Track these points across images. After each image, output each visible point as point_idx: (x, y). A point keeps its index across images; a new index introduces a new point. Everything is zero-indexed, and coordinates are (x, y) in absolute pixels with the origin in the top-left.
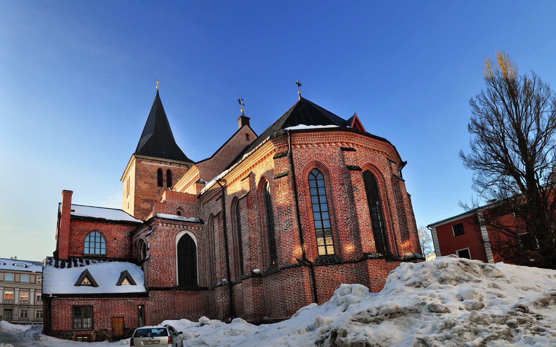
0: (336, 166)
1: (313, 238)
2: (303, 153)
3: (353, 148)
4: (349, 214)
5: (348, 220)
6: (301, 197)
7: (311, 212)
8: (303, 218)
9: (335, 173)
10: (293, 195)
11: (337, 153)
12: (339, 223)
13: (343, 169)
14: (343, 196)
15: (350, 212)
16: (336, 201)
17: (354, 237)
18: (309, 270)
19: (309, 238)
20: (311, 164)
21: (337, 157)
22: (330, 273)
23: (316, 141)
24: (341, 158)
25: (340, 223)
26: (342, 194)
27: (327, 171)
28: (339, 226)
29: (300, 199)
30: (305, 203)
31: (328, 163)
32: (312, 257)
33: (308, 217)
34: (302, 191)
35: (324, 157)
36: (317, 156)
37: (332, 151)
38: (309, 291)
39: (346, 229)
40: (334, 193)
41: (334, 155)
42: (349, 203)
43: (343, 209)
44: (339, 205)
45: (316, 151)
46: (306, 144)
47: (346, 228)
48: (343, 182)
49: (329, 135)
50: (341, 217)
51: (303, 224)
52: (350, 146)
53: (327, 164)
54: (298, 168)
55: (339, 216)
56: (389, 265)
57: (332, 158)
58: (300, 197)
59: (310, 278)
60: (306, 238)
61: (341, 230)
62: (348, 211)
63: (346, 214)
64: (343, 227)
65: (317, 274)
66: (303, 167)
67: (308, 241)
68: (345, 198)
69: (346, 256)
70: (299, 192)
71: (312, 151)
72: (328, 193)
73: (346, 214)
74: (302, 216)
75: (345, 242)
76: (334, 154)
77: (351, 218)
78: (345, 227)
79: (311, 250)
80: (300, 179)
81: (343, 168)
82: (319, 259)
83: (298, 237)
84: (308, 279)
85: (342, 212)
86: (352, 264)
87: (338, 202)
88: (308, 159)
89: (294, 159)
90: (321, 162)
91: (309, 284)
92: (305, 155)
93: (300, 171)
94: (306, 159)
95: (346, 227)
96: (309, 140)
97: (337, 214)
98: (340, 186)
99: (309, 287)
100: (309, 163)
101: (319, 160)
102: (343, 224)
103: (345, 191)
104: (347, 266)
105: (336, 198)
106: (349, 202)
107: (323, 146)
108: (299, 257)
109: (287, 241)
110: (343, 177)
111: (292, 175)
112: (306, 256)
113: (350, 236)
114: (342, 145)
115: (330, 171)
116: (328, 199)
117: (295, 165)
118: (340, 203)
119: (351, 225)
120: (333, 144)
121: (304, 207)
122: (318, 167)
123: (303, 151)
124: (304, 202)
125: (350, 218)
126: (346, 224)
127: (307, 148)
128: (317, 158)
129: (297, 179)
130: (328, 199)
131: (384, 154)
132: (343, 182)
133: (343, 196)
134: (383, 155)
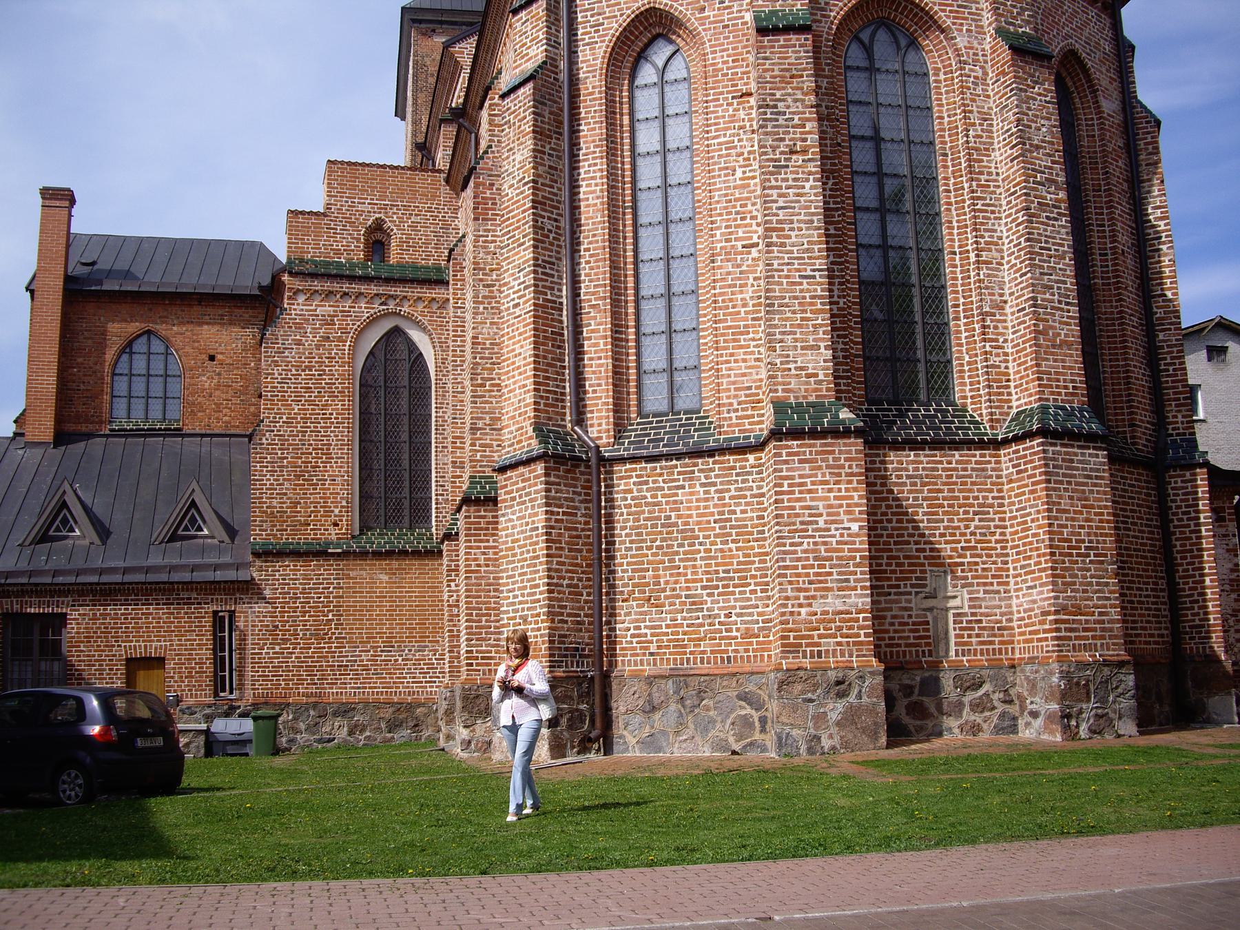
4: (754, 227)
5: (749, 253)
25: (720, 267)
34: (594, 141)
39: (740, 296)
43: (734, 207)
44: (720, 189)
47: (741, 292)
48: (746, 84)
54: (588, 44)
62: (755, 213)
63: (746, 226)
64: (730, 286)
66: (606, 35)
67: (596, 352)
73: (746, 226)
75: (732, 355)
78: (735, 286)
85: (728, 220)
87: (719, 176)
102: (729, 273)
103: (751, 126)
108: (550, 419)
110: (747, 66)
113: (754, 326)
118: (725, 182)
124: (596, 185)
126: (741, 273)
132: (746, 84)
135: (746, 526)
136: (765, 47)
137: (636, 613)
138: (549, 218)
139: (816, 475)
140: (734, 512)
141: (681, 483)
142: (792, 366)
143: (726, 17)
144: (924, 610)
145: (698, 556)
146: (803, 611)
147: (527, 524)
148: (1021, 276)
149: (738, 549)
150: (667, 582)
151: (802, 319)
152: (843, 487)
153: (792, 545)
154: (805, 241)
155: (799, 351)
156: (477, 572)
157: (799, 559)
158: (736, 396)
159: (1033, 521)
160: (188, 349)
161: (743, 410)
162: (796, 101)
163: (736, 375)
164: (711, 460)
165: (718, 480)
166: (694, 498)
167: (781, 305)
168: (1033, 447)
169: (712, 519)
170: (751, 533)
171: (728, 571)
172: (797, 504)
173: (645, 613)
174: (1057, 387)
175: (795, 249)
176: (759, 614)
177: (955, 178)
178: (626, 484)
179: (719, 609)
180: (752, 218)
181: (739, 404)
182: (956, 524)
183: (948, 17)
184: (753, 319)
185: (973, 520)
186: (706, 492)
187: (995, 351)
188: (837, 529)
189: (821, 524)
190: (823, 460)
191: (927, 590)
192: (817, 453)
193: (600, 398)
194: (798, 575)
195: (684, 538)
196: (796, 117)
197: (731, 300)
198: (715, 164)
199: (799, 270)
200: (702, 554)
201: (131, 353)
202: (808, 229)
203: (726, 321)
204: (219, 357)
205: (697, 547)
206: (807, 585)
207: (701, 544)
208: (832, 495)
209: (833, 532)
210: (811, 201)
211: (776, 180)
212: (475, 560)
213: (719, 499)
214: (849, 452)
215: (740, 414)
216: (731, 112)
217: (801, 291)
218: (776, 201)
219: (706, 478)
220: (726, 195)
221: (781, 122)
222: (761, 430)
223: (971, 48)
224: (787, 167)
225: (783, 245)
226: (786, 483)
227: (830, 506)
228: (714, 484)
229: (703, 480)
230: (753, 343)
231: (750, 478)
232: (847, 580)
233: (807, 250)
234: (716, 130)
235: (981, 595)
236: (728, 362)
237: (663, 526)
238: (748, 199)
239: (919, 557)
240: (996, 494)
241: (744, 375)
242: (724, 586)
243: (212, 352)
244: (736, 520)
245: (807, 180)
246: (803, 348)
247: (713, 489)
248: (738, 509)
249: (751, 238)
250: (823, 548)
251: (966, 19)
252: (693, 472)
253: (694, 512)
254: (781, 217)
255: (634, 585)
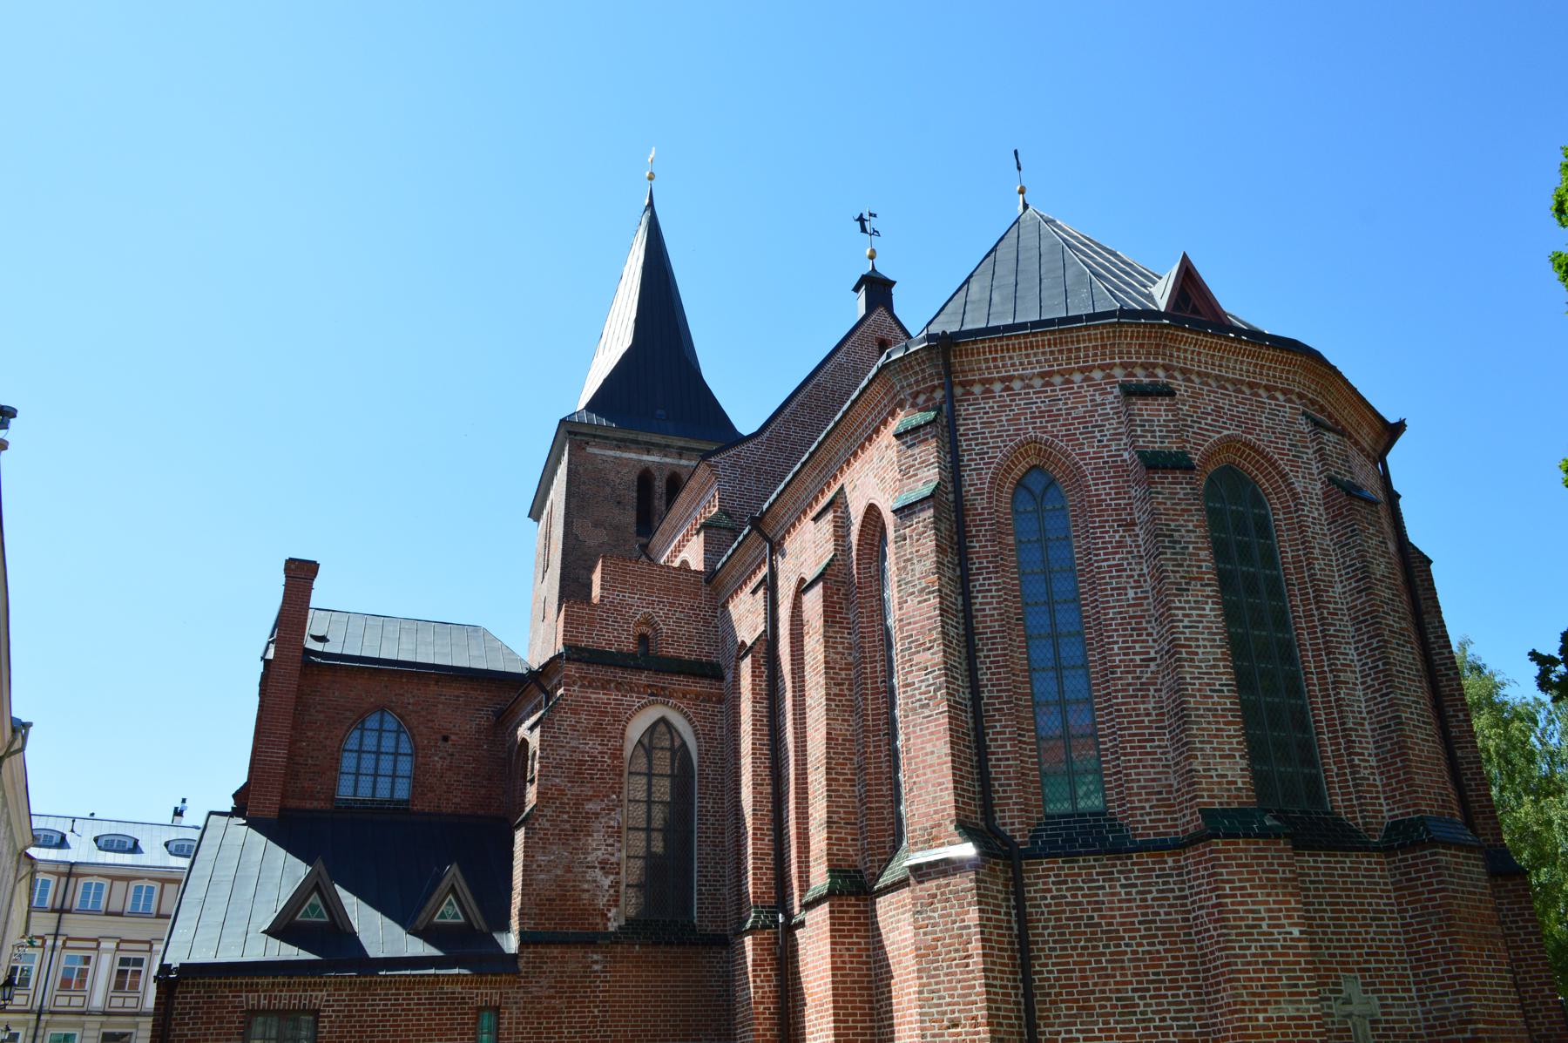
0: (1105, 454)
1: (1025, 743)
2: (991, 414)
3: (1166, 385)
4: (1151, 643)
5: (1148, 666)
6: (984, 579)
7: (1018, 636)
8: (988, 660)
9: (1103, 484)
10: (954, 570)
11: (1108, 407)
12: (1113, 679)
13: (1132, 464)
14: (1131, 570)
15: (1155, 637)
16: (1106, 590)
17: (1172, 738)
18: (1007, 872)
19: (1010, 739)
20: (1021, 453)
21: (1108, 419)
22: (1083, 889)
23: (1035, 368)
24: (1122, 423)
25: (1120, 679)
26: (1125, 563)
27: (1076, 474)
28: (1116, 691)
29: (978, 588)
30: (994, 600)
31: (1077, 445)
32: (1016, 820)
33: (1005, 655)
34: (987, 557)
35: (1063, 425)
36: (1041, 422)
37: (1091, 401)
38: (1002, 965)
39: (1142, 706)
40: (1096, 561)
41: (1099, 415)
42: (1151, 600)
43: (1130, 624)
44: (1114, 607)
45: (1036, 403)
46: (1002, 380)
47: (1144, 703)
48: (1129, 514)
49: (1078, 342)
50: (1122, 657)
51: (986, 686)
52: (1156, 376)
53: (1074, 450)
54: (974, 470)
55: (1116, 651)
56: (1320, 868)
57: (1092, 427)
58: (978, 580)
59: (1008, 907)
60: (996, 740)
61: (1123, 708)
62: (1150, 630)
63: (1143, 641)
64: (1132, 696)
65: (1036, 891)
66: (992, 463)
67: (1003, 753)
68: (1136, 578)
69: (1144, 822)
70: (977, 558)
71: (1022, 402)
72: (1081, 558)
73: (1143, 641)
74: (985, 653)
75: (1140, 760)
76: (1097, 411)
77: (1158, 661)
78: (1137, 696)
79: (1014, 791)
80: (980, 511)
81: (1129, 462)
82: (1045, 830)
83: (969, 735)
84: (999, 913)
85: (1125, 636)
86: (1166, 858)
87: (1112, 595)
88: (1007, 436)
89: (961, 435)
90: (1053, 441)
91: (1003, 935)
92: (998, 421)
93: (980, 479)
94: (1002, 436)
95: (1143, 696)
96: (1013, 365)
97: (1109, 643)
98: (1121, 533)
99: (1005, 950)
100: (1012, 447)
101: (1045, 436)
102: (1129, 684)
103: (1139, 552)
104: (1147, 863)
105: (1104, 578)
106: (1150, 595)
107: (1063, 383)
109: (926, 754)
110: (1130, 498)
111: (951, 497)
112: (998, 815)
113: (1159, 734)
114: (1126, 376)
115: (1086, 476)
116: (1081, 582)
117: (966, 458)
118: (1118, 601)
119: (1160, 690)
120: (1097, 375)
121: (993, 615)
122: (1045, 463)
123: (991, 404)
124: (992, 597)
125: (1154, 659)
126: (1141, 684)
127: (1005, 394)
128: (1040, 428)
129: (968, 510)
130: (1081, 582)
131: (1294, 397)
132: (1129, 514)
133: (1131, 570)
134: (1287, 405)
135: (1172, 928)
136: (1156, 483)
137: (1066, 1016)
138: (952, 626)
139: (1254, 880)
140: (1158, 914)
141: (1101, 883)
142: (1213, 773)
143: (1105, 454)
144: (1344, 1016)
145: (1126, 958)
146: (1261, 1016)
147: (954, 922)
148: (1382, 696)
149: (1166, 951)
150: (1095, 984)
151: (1217, 730)
152: (1279, 891)
153: (1241, 948)
154: (1211, 657)
155: (1218, 760)
156: (844, 969)
157: (1249, 963)
158: (1147, 800)
159: (1434, 928)
160: (421, 727)
161: (1156, 813)
162: (1188, 531)
163: (1146, 780)
164: (1129, 862)
165: (1139, 882)
166: (1116, 898)
167: (1196, 716)
168: (1426, 856)
169: (1136, 920)
170: (1178, 936)
171: (1157, 974)
172: (1241, 908)
173: (1074, 1016)
174: (1430, 799)
175: (1203, 665)
176: (1196, 1019)
177: (1304, 606)
178: (1044, 883)
179: (1153, 1012)
180: (1148, 635)
181: (1151, 807)
182: (1357, 929)
183: (1286, 465)
184: (1157, 728)
185: (1371, 926)
186: (1127, 893)
187: (1363, 764)
188: (1279, 933)
189: (1265, 928)
190: (1258, 865)
191: (1343, 995)
192: (1254, 858)
193: (1011, 798)
194: (1251, 979)
195: (1109, 939)
196: (1191, 546)
197: (1134, 709)
198: (1106, 584)
199: (1208, 685)
200: (1129, 956)
201: (363, 729)
202: (1212, 647)
203: (1131, 728)
204: (453, 737)
205: (1123, 948)
206: (1260, 990)
207: (1127, 945)
208: (1271, 899)
209: (1276, 936)
210: (1212, 622)
211: (1180, 601)
212: (841, 956)
213: (1142, 900)
214: (1280, 858)
215: (1153, 817)
216: (1117, 538)
217: (1213, 703)
218: (1182, 621)
219: (1126, 879)
220: (1120, 613)
221: (1178, 550)
222: (1176, 833)
223: (1308, 493)
224: (1188, 590)
225: (1192, 660)
226: (1227, 886)
227: (1270, 910)
228: (1135, 885)
229: (1123, 882)
230: (1159, 751)
231: (1171, 880)
232: (1296, 986)
233: (1214, 667)
234: (1105, 554)
235: (1390, 1002)
236: (1137, 767)
237: (1086, 926)
238: (1143, 617)
239: (1331, 963)
240: (1385, 901)
241: (1153, 780)
242: (1156, 989)
243: (445, 733)
244: (1161, 921)
245: (1207, 603)
246: (1221, 757)
247: (1134, 890)
248: (1162, 911)
249: (1148, 653)
250: (1269, 952)
251: (1300, 467)
252: (1112, 873)
253: (1117, 913)
254: (1188, 635)
255: (1061, 986)
